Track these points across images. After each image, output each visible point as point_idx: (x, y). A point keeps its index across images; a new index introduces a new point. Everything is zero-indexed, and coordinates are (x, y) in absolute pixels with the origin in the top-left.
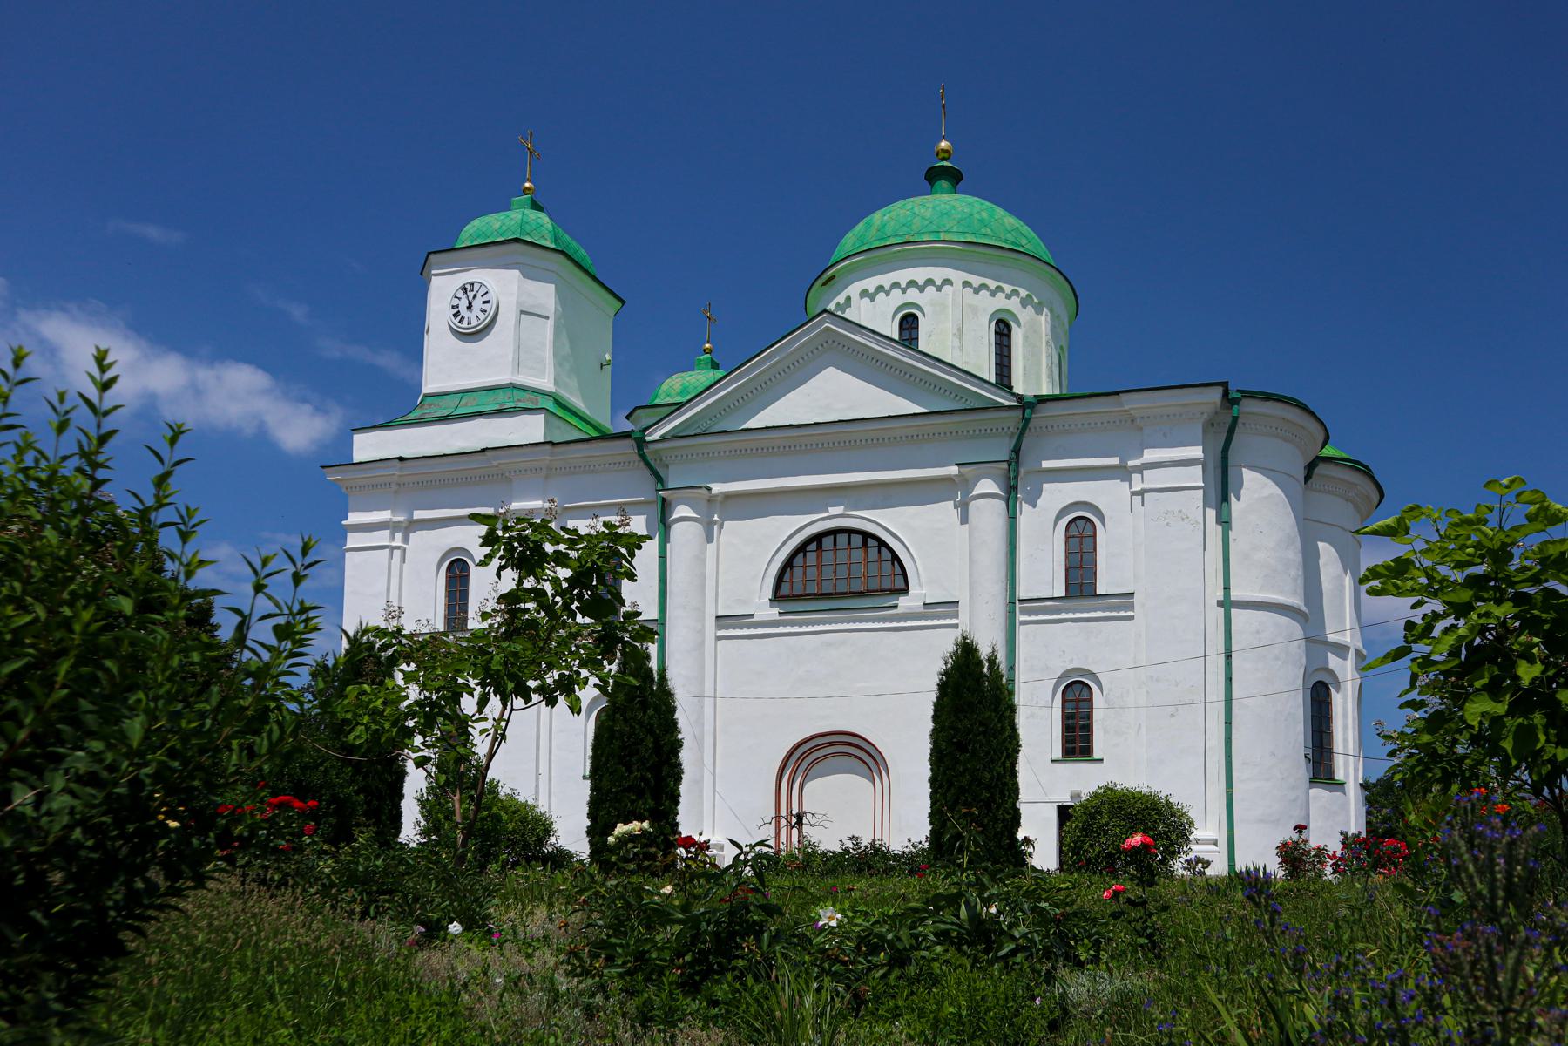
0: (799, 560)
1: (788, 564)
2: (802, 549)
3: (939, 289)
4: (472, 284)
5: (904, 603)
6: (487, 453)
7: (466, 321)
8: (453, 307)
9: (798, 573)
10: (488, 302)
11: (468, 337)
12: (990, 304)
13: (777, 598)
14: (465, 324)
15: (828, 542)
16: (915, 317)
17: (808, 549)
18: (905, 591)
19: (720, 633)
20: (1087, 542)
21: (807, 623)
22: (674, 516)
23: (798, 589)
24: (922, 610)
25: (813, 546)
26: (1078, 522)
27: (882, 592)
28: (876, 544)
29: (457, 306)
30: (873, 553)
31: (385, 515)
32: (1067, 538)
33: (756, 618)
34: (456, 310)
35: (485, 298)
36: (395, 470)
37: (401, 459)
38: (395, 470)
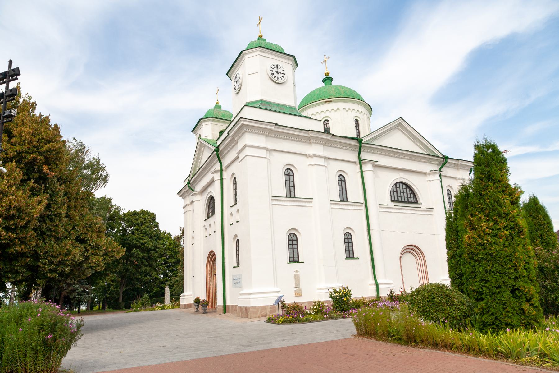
2: (393, 187)
7: (276, 77)
8: (271, 71)
10: (284, 74)
15: (398, 185)
27: (411, 203)
29: (272, 71)
30: (408, 190)
34: (272, 72)
37: (276, 124)
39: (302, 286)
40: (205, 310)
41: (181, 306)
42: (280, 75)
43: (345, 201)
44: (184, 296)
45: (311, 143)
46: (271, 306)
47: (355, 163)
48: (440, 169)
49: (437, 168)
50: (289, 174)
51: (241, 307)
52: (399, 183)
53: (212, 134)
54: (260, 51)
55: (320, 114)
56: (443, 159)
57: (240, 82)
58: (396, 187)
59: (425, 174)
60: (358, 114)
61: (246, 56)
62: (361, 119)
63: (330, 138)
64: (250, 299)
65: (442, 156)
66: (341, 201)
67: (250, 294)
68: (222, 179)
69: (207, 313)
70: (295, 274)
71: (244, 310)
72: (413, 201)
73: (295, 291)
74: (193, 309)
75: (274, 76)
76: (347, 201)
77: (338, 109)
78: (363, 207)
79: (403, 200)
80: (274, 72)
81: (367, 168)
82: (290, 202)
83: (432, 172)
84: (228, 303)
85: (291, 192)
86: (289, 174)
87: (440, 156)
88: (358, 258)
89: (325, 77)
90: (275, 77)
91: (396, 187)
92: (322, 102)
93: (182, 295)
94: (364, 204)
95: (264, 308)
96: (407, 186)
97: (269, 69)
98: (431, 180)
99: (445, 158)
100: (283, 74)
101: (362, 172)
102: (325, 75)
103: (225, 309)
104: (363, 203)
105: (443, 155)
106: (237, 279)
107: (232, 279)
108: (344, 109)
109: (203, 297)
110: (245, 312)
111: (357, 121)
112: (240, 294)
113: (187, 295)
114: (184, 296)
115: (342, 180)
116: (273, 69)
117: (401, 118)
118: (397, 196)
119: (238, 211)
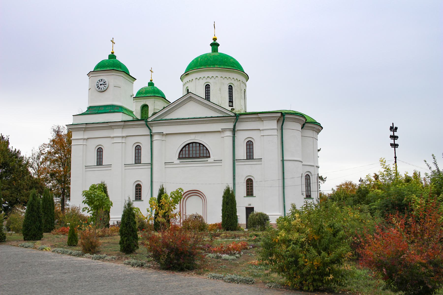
0: (184, 149)
1: (182, 150)
2: (185, 146)
3: (215, 79)
5: (209, 160)
8: (97, 85)
9: (184, 152)
10: (106, 84)
12: (227, 83)
13: (179, 158)
15: (191, 145)
16: (209, 85)
17: (186, 147)
18: (209, 157)
20: (251, 146)
22: (154, 139)
23: (184, 156)
25: (187, 146)
26: (249, 142)
27: (204, 157)
28: (202, 146)
32: (247, 145)
34: (98, 86)
35: (105, 83)
37: (86, 124)
43: (139, 163)
45: (113, 129)
47: (149, 135)
48: (235, 126)
49: (231, 126)
50: (100, 151)
52: (192, 143)
53: (136, 109)
54: (92, 74)
56: (235, 117)
58: (189, 147)
59: (219, 131)
60: (209, 80)
63: (123, 124)
65: (234, 115)
66: (135, 163)
72: (205, 155)
76: (140, 163)
79: (194, 156)
81: (156, 137)
82: (100, 168)
83: (223, 130)
85: (100, 162)
86: (100, 151)
88: (143, 201)
89: (212, 41)
91: (189, 147)
96: (200, 144)
97: (96, 83)
98: (223, 136)
101: (152, 142)
105: (235, 114)
115: (138, 149)
116: (99, 83)
118: (189, 154)
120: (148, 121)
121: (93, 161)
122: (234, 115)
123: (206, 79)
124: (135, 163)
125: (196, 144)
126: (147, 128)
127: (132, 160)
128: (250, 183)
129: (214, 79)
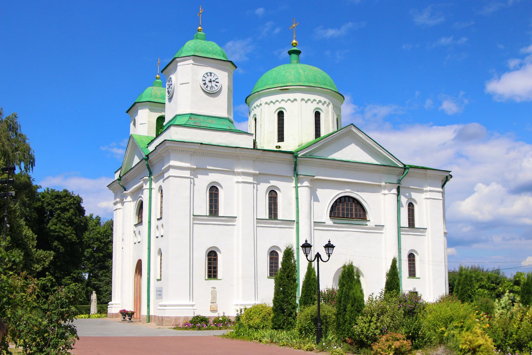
2: (336, 201)
4: (211, 73)
6: (237, 149)
10: (218, 82)
11: (209, 94)
14: (209, 89)
17: (337, 201)
19: (315, 228)
21: (340, 227)
24: (374, 227)
29: (205, 81)
31: (187, 165)
33: (326, 224)
34: (204, 82)
35: (217, 81)
36: (197, 147)
37: (201, 144)
38: (197, 147)
39: (218, 302)
40: (130, 319)
41: (109, 316)
42: (214, 84)
44: (112, 304)
46: (184, 317)
48: (399, 182)
51: (158, 316)
53: (149, 121)
55: (274, 103)
57: (172, 88)
60: (320, 106)
61: (179, 64)
62: (324, 111)
64: (165, 309)
65: (402, 166)
67: (165, 306)
68: (151, 189)
69: (132, 322)
70: (212, 290)
71: (161, 319)
73: (211, 305)
74: (121, 318)
75: (206, 86)
77: (295, 100)
78: (295, 226)
80: (207, 82)
84: (152, 313)
87: (400, 166)
90: (207, 87)
92: (277, 90)
93: (110, 303)
94: (295, 223)
95: (177, 319)
97: (200, 78)
99: (405, 167)
100: (216, 82)
101: (297, 187)
102: (292, 45)
103: (149, 318)
104: (294, 221)
105: (405, 166)
106: (159, 291)
107: (155, 291)
108: (303, 100)
109: (130, 308)
110: (161, 320)
111: (317, 115)
112: (159, 305)
113: (116, 304)
114: (112, 304)
115: (273, 196)
116: (206, 78)
117: (352, 124)
119: (162, 226)
120: (299, 156)
121: (203, 208)
122: (402, 166)
123: (318, 103)
124: (270, 218)
125: (349, 199)
126: (293, 166)
127: (264, 214)
128: (411, 257)
129: (304, 102)
